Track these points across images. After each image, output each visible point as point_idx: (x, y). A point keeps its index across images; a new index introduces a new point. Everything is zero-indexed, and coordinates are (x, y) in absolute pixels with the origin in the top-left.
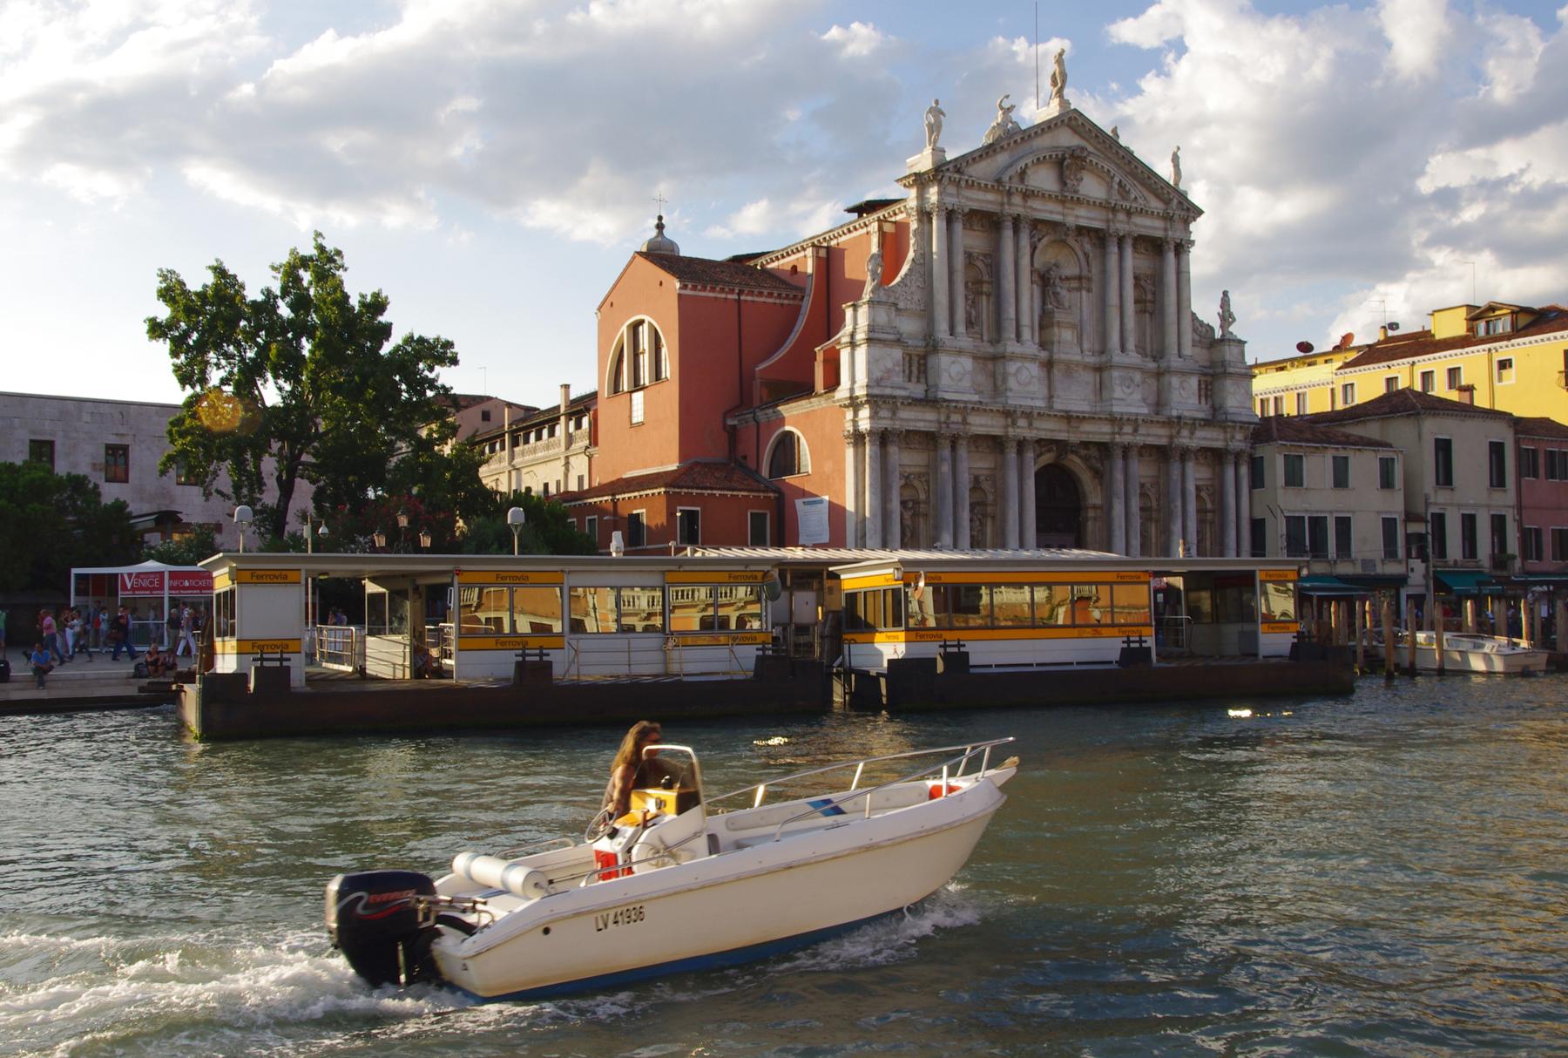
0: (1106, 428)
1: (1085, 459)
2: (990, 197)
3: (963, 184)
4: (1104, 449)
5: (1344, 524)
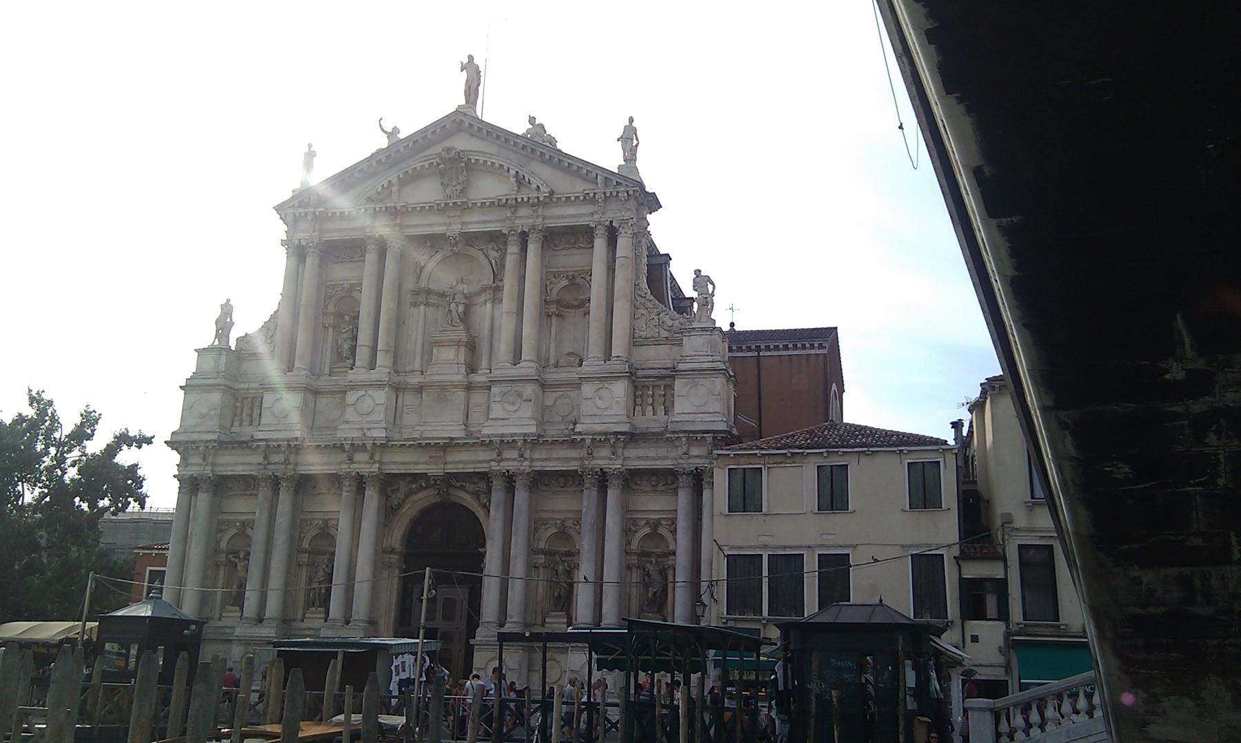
0: (484, 455)
1: (476, 494)
3: (310, 217)
4: (485, 476)
5: (836, 570)
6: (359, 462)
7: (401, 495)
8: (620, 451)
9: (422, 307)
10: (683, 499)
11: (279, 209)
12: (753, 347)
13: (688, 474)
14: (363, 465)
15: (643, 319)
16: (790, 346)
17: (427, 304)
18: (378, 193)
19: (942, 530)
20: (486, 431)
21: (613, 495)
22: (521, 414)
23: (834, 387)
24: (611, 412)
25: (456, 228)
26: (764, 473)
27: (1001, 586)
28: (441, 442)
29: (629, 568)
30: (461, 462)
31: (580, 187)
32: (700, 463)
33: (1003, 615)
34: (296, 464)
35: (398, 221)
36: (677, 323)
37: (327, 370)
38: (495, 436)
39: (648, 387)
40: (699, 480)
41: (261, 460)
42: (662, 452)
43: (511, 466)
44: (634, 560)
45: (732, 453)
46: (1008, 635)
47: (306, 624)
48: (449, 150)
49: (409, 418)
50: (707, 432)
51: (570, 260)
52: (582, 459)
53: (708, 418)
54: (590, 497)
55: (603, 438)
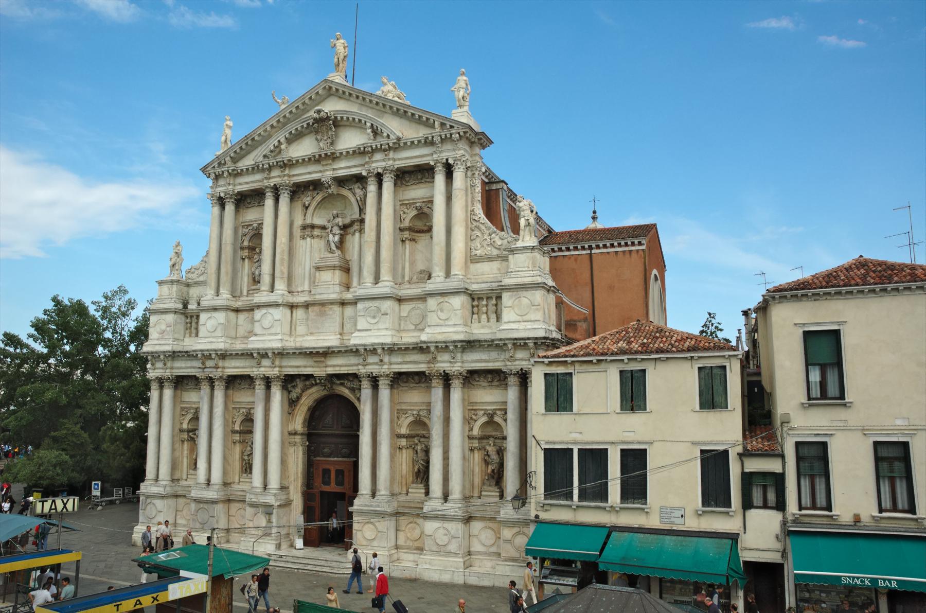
0: (353, 360)
1: (352, 390)
2: (258, 177)
3: (226, 174)
4: (355, 376)
6: (265, 367)
7: (298, 390)
8: (459, 356)
9: (308, 239)
10: (512, 394)
11: (204, 170)
12: (586, 246)
13: (515, 375)
14: (267, 369)
15: (478, 240)
16: (616, 244)
17: (312, 237)
18: (272, 151)
19: (726, 428)
20: (354, 342)
21: (456, 395)
22: (381, 326)
23: (655, 272)
24: (450, 323)
25: (326, 174)
26: (574, 378)
27: (779, 480)
28: (321, 351)
29: (472, 450)
30: (338, 366)
31: (421, 132)
32: (525, 365)
33: (780, 506)
34: (224, 368)
35: (287, 172)
36: (505, 241)
37: (245, 293)
38: (360, 345)
39: (482, 298)
40: (524, 378)
41: (201, 365)
42: (494, 355)
43: (375, 369)
44: (476, 444)
45: (546, 360)
46: (784, 523)
47: (240, 487)
48: (319, 112)
49: (301, 329)
50: (528, 339)
51: (416, 192)
52: (429, 362)
53: (529, 326)
54: (438, 392)
55: (444, 345)
